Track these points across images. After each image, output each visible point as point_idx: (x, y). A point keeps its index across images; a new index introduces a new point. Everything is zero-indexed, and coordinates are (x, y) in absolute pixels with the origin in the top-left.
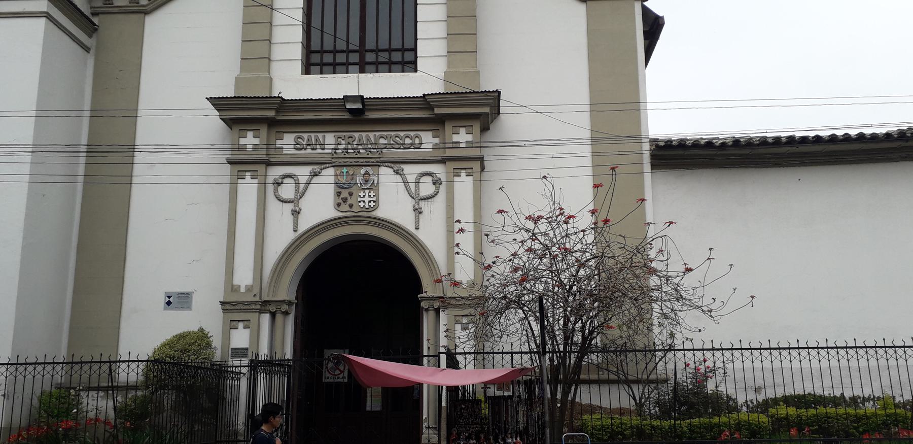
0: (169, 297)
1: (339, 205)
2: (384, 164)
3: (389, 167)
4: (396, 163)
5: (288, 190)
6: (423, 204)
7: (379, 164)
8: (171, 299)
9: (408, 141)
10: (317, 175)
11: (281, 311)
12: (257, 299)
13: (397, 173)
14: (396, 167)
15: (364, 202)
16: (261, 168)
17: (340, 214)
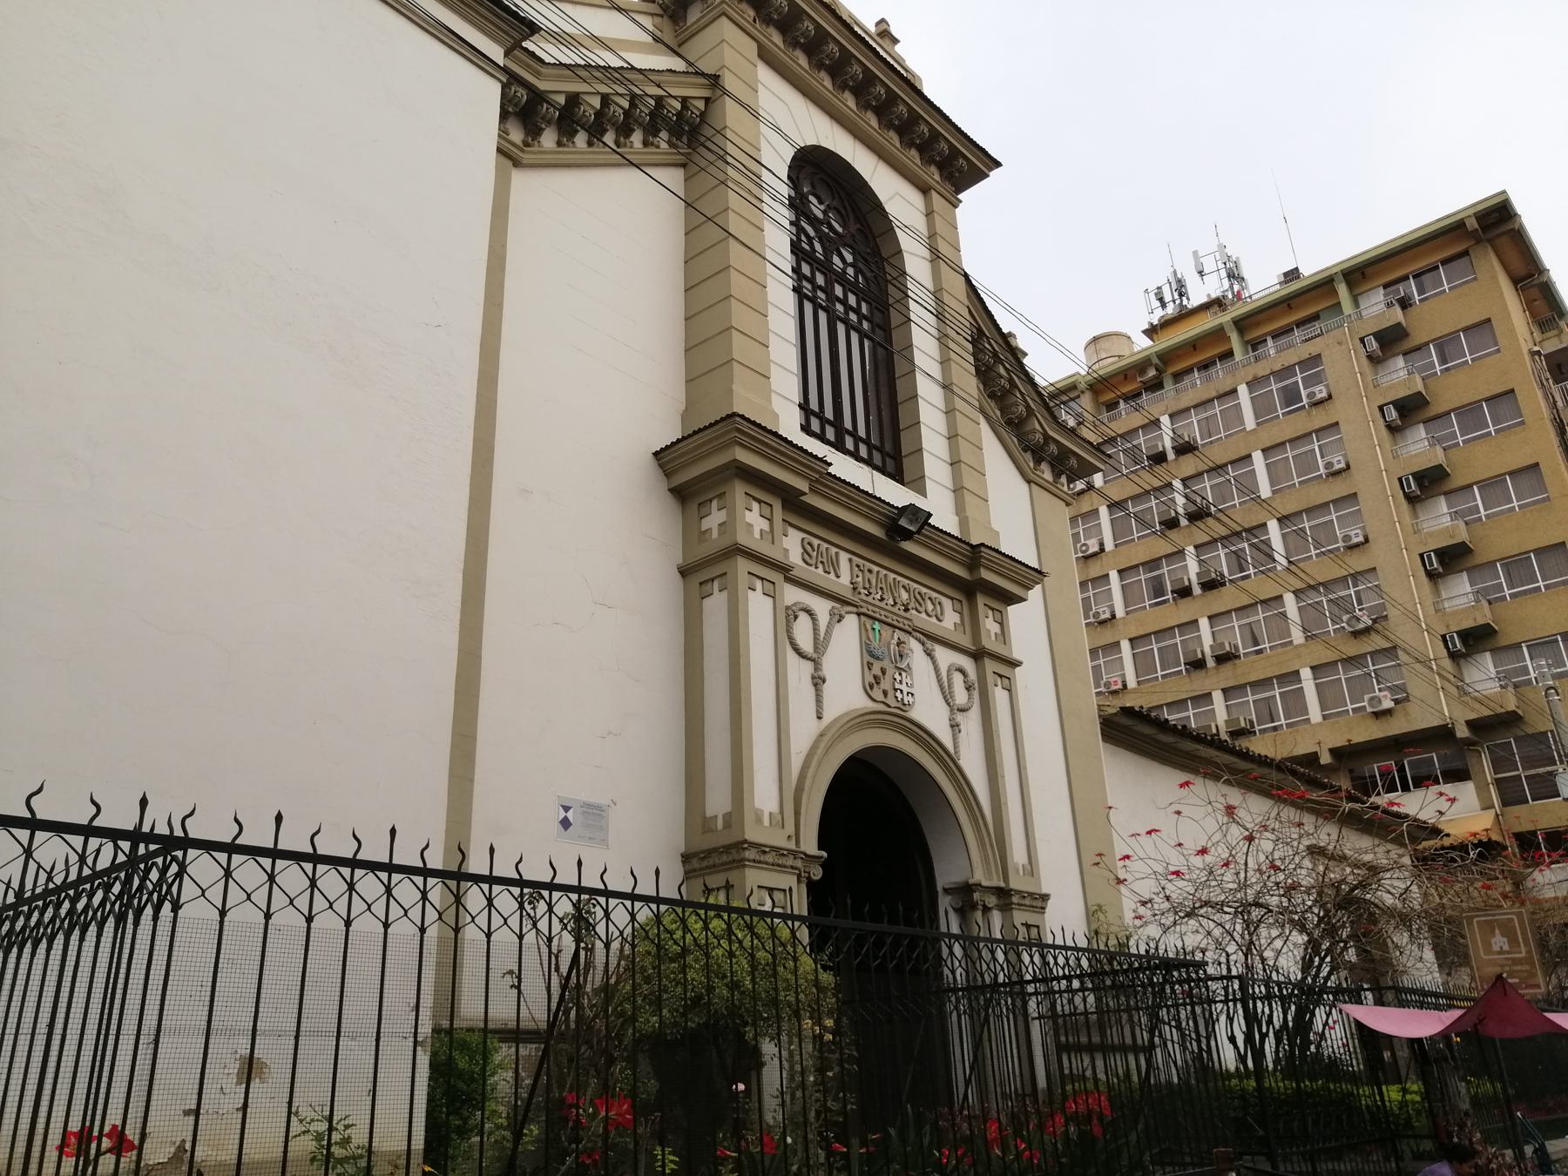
0: (566, 809)
1: (871, 687)
2: (914, 633)
3: (919, 641)
4: (930, 638)
5: (803, 631)
6: (959, 717)
7: (910, 630)
8: (570, 815)
9: (930, 607)
10: (839, 621)
11: (809, 878)
12: (792, 846)
13: (929, 655)
14: (929, 644)
15: (901, 691)
16: (777, 577)
17: (872, 706)
